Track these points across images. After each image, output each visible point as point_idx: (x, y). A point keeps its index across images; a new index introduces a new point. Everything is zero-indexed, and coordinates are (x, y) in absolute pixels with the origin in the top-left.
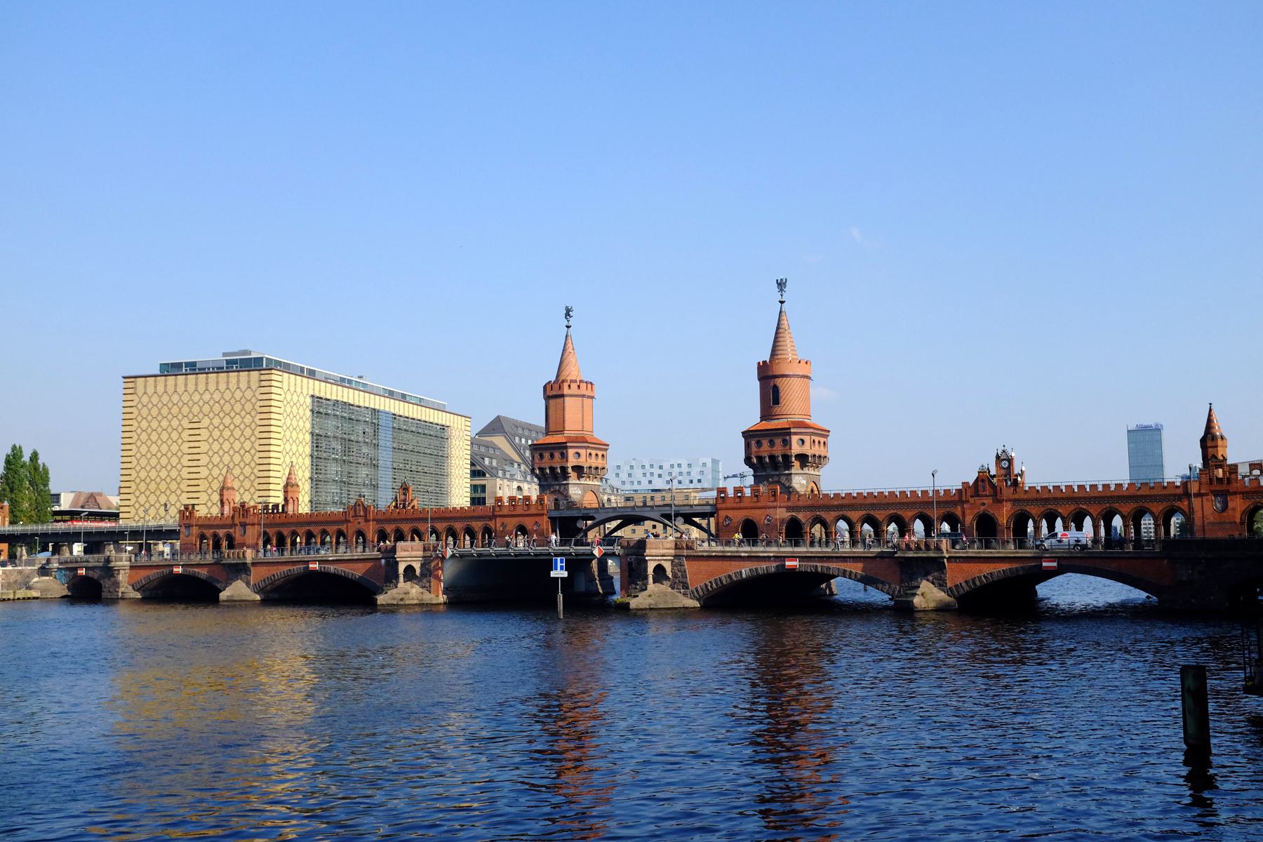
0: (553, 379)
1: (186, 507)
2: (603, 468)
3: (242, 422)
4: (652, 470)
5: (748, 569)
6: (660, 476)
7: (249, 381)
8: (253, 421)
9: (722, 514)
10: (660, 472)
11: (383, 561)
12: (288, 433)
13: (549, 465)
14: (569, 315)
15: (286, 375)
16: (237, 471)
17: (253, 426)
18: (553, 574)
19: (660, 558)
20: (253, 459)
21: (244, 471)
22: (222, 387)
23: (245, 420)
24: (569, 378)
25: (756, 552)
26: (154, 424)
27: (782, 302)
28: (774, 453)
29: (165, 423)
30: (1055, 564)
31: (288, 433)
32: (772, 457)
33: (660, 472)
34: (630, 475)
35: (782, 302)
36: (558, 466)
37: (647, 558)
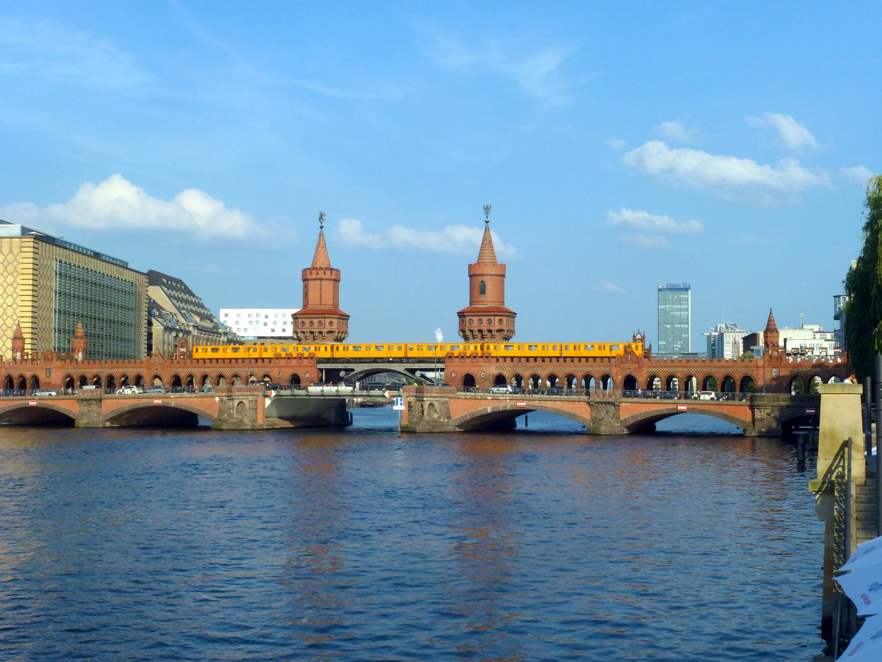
0: (310, 266)
2: (346, 333)
3: (5, 281)
4: (258, 319)
5: (491, 407)
6: (265, 324)
7: (11, 248)
8: (15, 281)
9: (450, 369)
10: (266, 320)
11: (217, 399)
12: (41, 291)
13: (309, 330)
14: (322, 219)
15: (40, 243)
17: (15, 285)
18: (395, 408)
19: (432, 399)
20: (15, 313)
21: (7, 322)
23: (8, 280)
24: (324, 266)
27: (487, 222)
28: (481, 328)
30: (685, 408)
31: (41, 291)
33: (266, 320)
34: (237, 323)
35: (487, 222)
36: (317, 331)
37: (425, 399)
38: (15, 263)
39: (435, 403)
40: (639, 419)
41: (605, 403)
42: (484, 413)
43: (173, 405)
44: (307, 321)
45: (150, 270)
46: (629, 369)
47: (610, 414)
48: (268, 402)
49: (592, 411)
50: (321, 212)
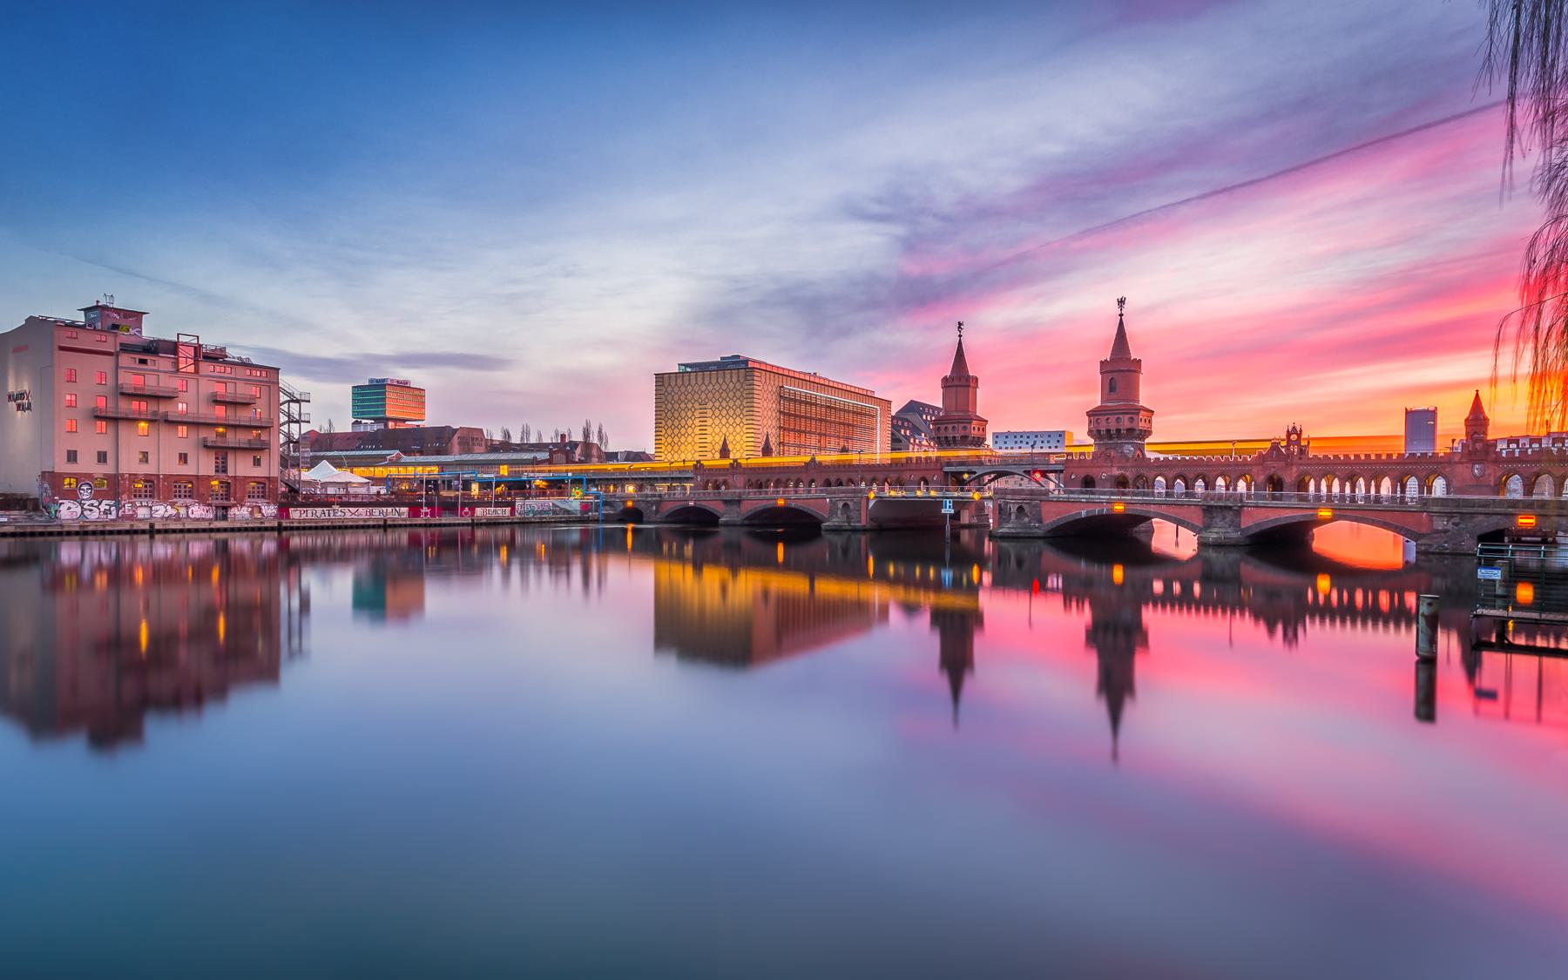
1: (698, 462)
6: (1027, 443)
11: (828, 500)
16: (730, 438)
18: (943, 511)
22: (721, 381)
25: (1092, 499)
26: (676, 406)
29: (683, 406)
32: (1108, 431)
38: (742, 390)
39: (1025, 506)
40: (1265, 527)
41: (1221, 507)
42: (1078, 517)
43: (793, 505)
44: (943, 427)
45: (912, 402)
46: (1274, 467)
47: (1227, 520)
48: (871, 504)
49: (1204, 517)
50: (959, 323)
